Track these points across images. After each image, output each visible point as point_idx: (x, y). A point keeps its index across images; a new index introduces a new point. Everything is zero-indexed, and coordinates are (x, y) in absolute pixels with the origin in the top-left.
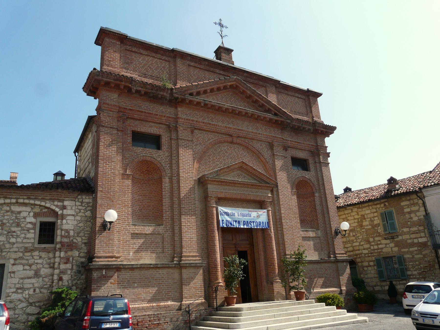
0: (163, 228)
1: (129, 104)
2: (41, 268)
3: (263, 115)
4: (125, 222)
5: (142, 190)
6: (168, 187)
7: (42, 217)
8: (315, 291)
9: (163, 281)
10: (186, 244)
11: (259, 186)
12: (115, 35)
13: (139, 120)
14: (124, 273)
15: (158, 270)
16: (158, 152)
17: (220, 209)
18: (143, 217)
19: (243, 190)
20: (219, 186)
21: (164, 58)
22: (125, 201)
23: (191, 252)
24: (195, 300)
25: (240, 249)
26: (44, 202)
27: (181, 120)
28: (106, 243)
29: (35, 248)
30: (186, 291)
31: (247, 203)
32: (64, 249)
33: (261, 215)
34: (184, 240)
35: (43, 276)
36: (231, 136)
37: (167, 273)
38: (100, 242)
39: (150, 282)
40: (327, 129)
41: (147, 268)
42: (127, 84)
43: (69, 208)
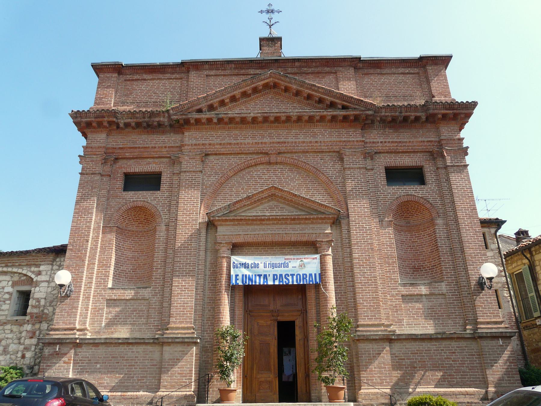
0: (151, 290)
1: (121, 142)
2: (10, 344)
3: (318, 114)
4: (101, 286)
5: (139, 245)
6: (164, 236)
7: (19, 285)
8: (418, 390)
9: (137, 363)
10: (177, 311)
11: (306, 219)
12: (109, 68)
13: (133, 158)
14: (85, 350)
15: (131, 347)
16: (155, 194)
17: (235, 259)
18: (137, 279)
19: (277, 229)
20: (236, 227)
21: (174, 76)
22: (103, 260)
23: (183, 322)
24: (173, 392)
25: (281, 319)
26: (21, 268)
27: (186, 147)
28: (68, 312)
29: (8, 320)
30: (165, 378)
31: (291, 248)
32: (32, 321)
33: (309, 263)
34: (174, 306)
35: (11, 353)
36: (266, 154)
37: (144, 352)
38: (61, 312)
39: (118, 363)
40: (457, 109)
41: (116, 343)
42: (111, 119)
43: (44, 273)
